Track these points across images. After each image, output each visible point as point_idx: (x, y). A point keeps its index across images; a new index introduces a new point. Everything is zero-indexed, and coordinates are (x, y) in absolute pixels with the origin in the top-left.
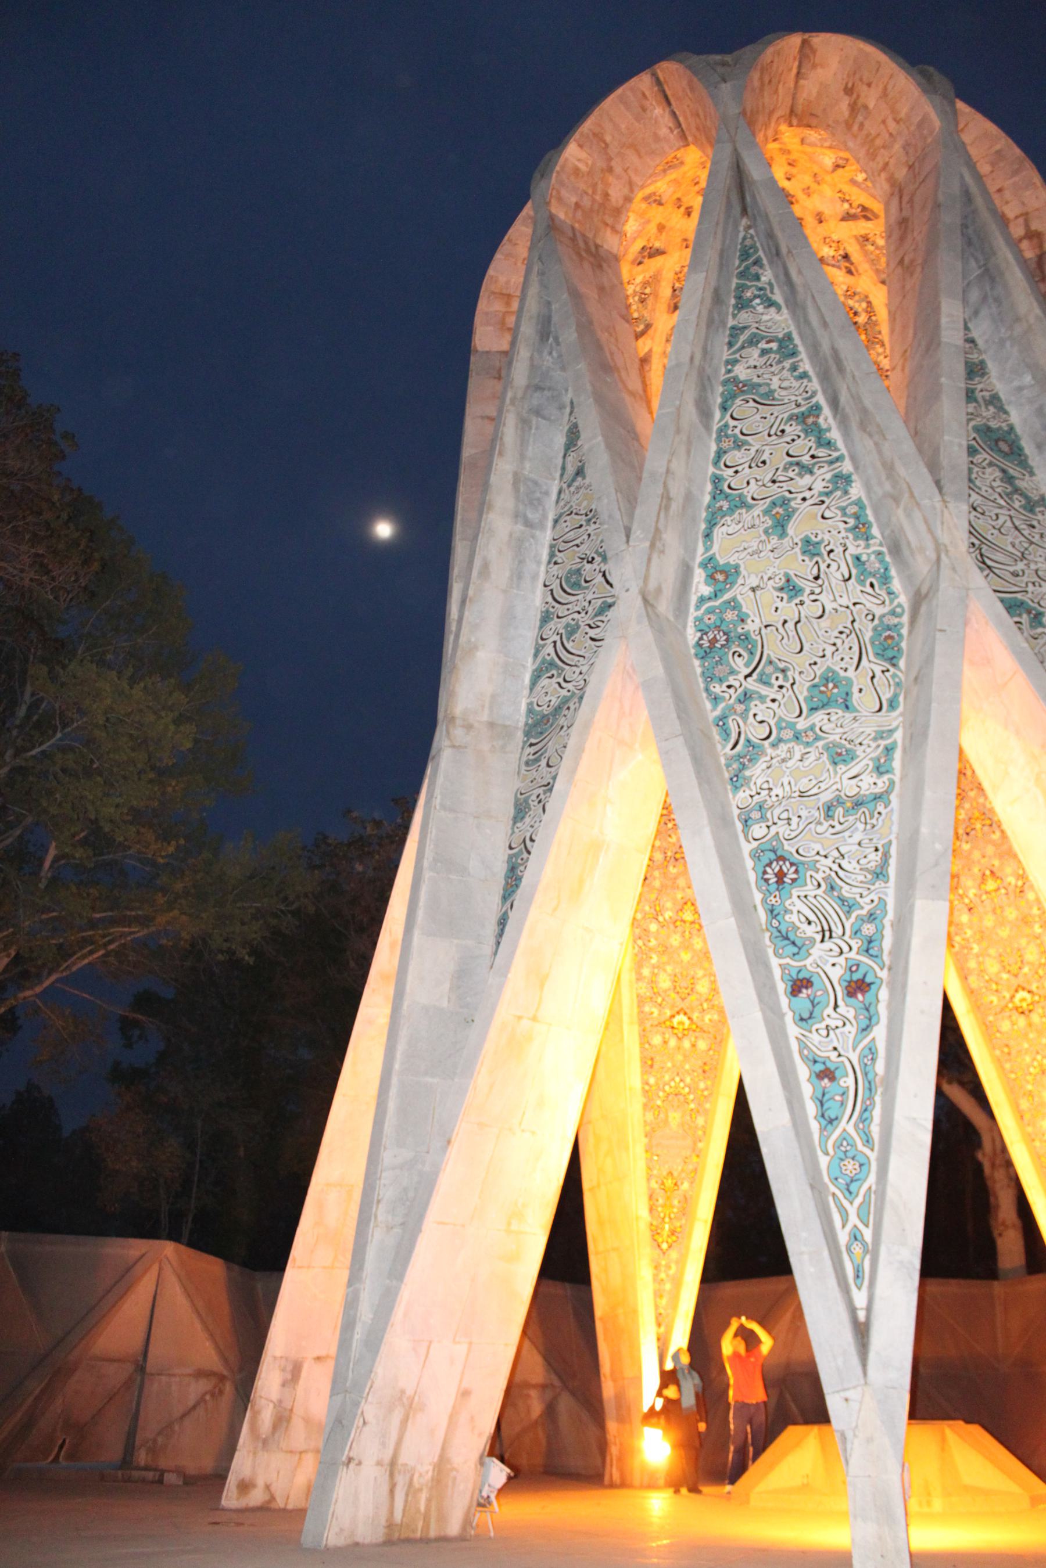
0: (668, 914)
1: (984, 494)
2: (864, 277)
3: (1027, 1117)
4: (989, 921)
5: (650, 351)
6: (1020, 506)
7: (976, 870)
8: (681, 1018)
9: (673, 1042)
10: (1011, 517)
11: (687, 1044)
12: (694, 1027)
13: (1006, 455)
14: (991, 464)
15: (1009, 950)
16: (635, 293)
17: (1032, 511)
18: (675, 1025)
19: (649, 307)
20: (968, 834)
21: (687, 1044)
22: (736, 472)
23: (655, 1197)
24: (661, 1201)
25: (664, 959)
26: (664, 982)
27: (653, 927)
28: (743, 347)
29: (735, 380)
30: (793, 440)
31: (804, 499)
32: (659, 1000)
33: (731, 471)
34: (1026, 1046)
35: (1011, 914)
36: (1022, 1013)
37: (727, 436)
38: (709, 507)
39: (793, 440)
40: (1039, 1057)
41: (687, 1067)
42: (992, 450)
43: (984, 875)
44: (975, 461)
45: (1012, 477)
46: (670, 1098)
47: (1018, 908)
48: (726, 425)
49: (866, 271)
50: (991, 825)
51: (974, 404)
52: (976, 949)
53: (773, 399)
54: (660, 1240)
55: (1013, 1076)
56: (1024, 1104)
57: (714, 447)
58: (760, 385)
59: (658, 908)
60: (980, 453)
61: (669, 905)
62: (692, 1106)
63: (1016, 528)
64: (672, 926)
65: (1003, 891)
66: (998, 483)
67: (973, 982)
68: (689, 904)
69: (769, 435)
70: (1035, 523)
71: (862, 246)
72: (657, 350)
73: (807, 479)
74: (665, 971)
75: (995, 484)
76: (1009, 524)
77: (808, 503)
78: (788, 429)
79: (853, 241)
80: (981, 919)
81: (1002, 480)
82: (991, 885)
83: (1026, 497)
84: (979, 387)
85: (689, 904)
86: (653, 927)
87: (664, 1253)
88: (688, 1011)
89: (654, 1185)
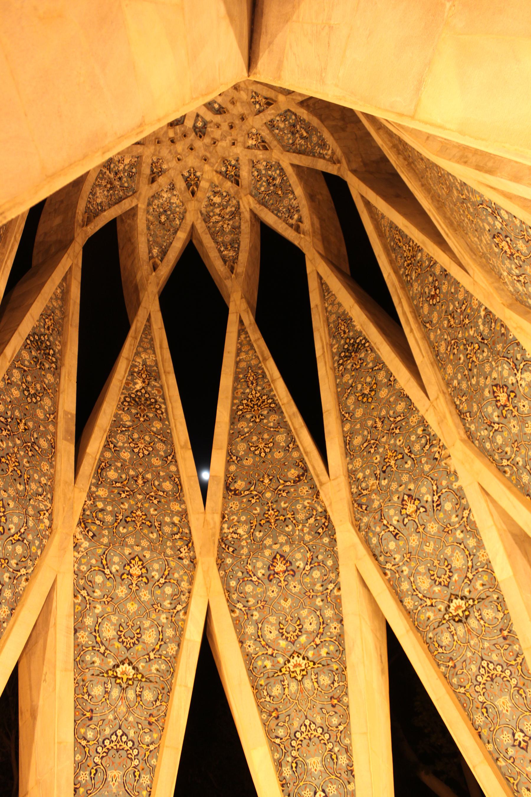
0: (114, 568)
2: (275, 151)
3: (485, 732)
4: (414, 541)
5: (137, 206)
7: (395, 499)
8: (126, 667)
9: (115, 692)
11: (131, 694)
12: (139, 676)
15: (436, 563)
16: (124, 170)
18: (119, 676)
19: (136, 182)
20: (384, 472)
21: (131, 694)
25: (109, 609)
26: (108, 632)
27: (99, 579)
32: (102, 649)
34: (469, 654)
35: (433, 528)
36: (460, 621)
40: (484, 663)
41: (131, 719)
43: (403, 500)
46: (111, 753)
47: (437, 521)
49: (275, 146)
50: (403, 458)
52: (406, 570)
55: (462, 690)
56: (479, 719)
59: (104, 562)
61: (116, 559)
64: (119, 580)
65: (422, 510)
67: (409, 602)
68: (137, 559)
71: (271, 131)
72: (142, 206)
74: (110, 620)
79: (264, 128)
80: (407, 541)
82: (411, 508)
85: (137, 559)
86: (99, 579)
88: (132, 660)
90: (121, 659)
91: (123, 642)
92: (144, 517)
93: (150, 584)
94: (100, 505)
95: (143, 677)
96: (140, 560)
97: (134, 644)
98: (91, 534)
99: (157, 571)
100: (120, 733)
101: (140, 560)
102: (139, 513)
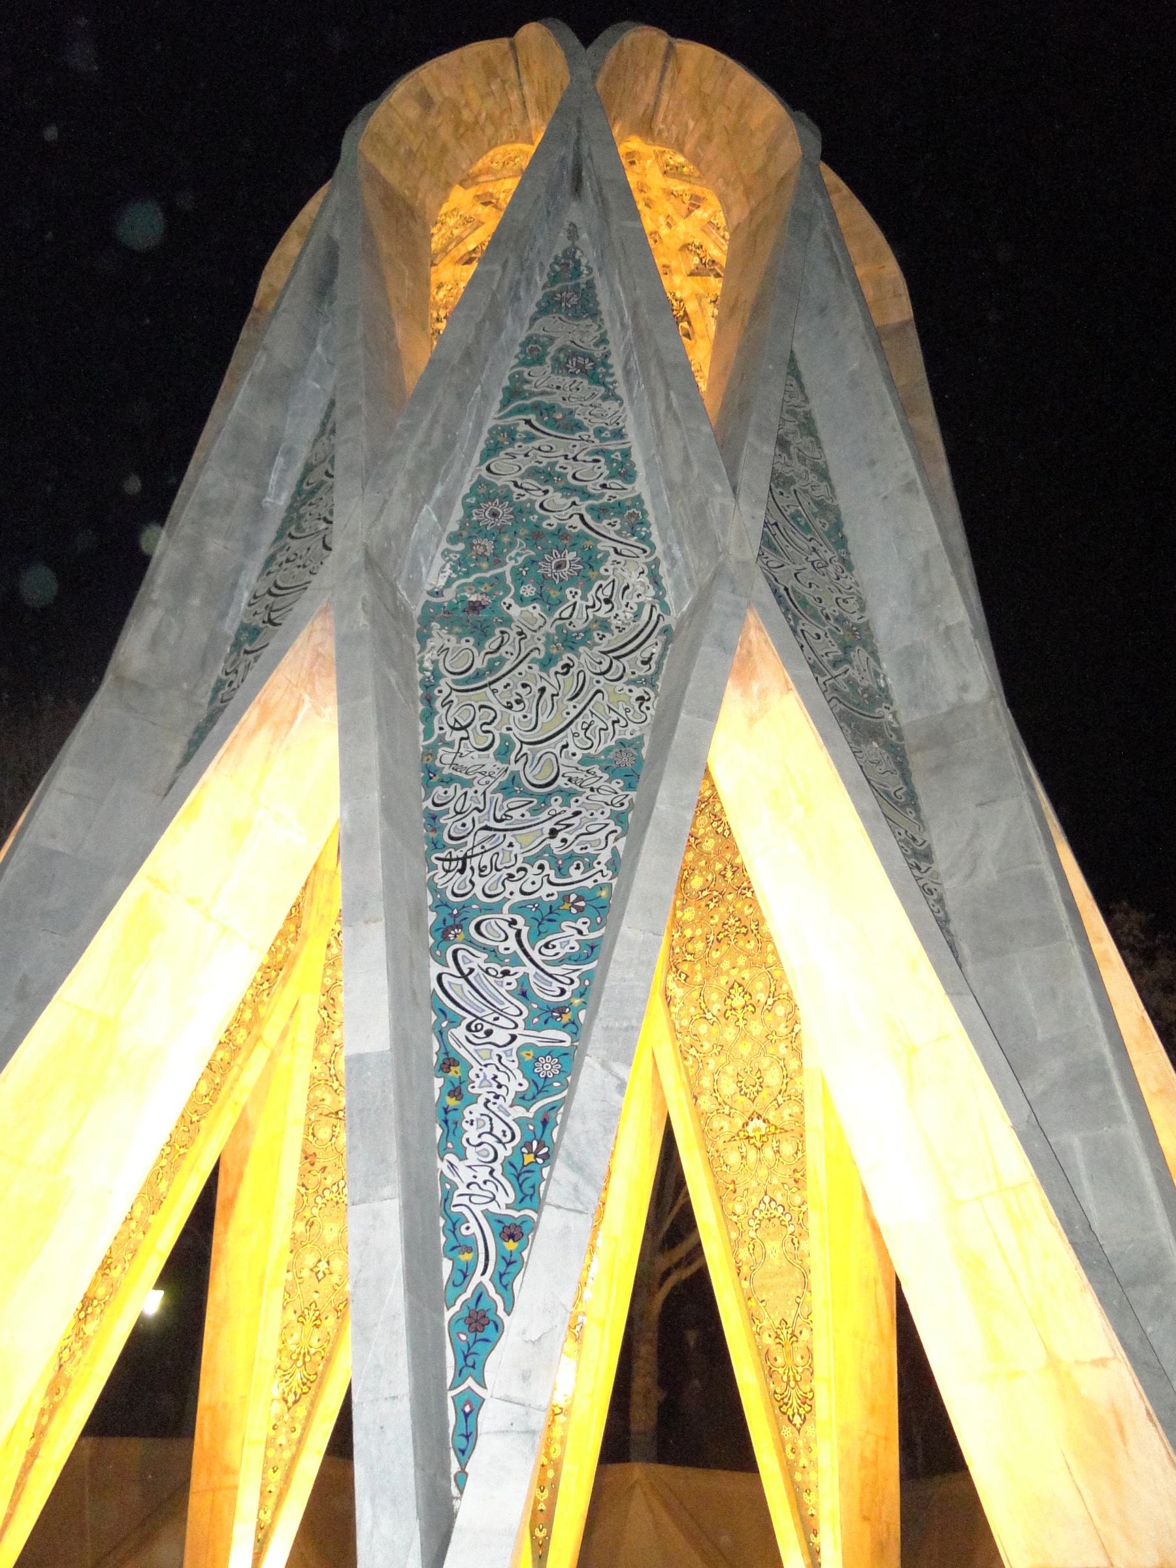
0: (715, 1009)
9: (752, 1155)
11: (768, 1152)
12: (772, 1129)
18: (751, 1135)
23: (772, 1355)
24: (780, 1361)
25: (722, 1059)
26: (728, 1087)
41: (775, 1181)
46: (764, 1224)
54: (790, 1413)
59: (703, 1006)
62: (791, 1229)
64: (723, 1020)
68: (736, 986)
85: (736, 986)
86: (703, 1028)
87: (799, 1430)
88: (761, 1112)
89: (767, 1340)
90: (748, 1115)
91: (746, 1094)
92: (737, 924)
93: (758, 1011)
94: (688, 933)
95: (776, 1128)
96: (740, 985)
97: (758, 1092)
98: (683, 976)
99: (761, 991)
100: (767, 1199)
101: (740, 985)
102: (732, 921)
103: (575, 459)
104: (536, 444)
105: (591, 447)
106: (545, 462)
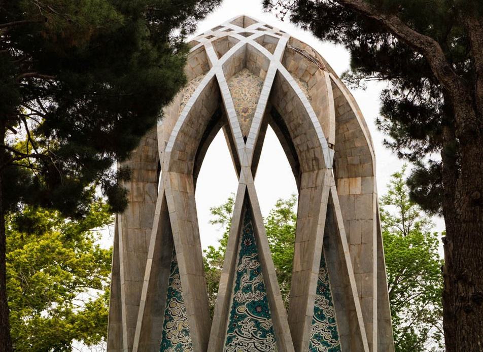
1: (245, 336)
6: (259, 336)
10: (254, 342)
13: (259, 313)
14: (252, 320)
17: (264, 336)
22: (169, 331)
28: (174, 274)
29: (171, 290)
30: (185, 320)
31: (186, 346)
33: (167, 331)
37: (168, 315)
38: (162, 344)
39: (185, 320)
42: (253, 313)
44: (244, 322)
45: (260, 323)
48: (168, 309)
51: (250, 293)
53: (181, 301)
57: (164, 319)
58: (178, 293)
60: (248, 316)
63: (255, 347)
66: (252, 328)
69: (179, 317)
70: (265, 342)
73: (187, 338)
75: (250, 330)
76: (253, 346)
77: (187, 347)
78: (184, 315)
81: (254, 327)
83: (263, 330)
84: (254, 282)
103: (324, 331)
104: (315, 325)
105: (328, 326)
106: (318, 331)
